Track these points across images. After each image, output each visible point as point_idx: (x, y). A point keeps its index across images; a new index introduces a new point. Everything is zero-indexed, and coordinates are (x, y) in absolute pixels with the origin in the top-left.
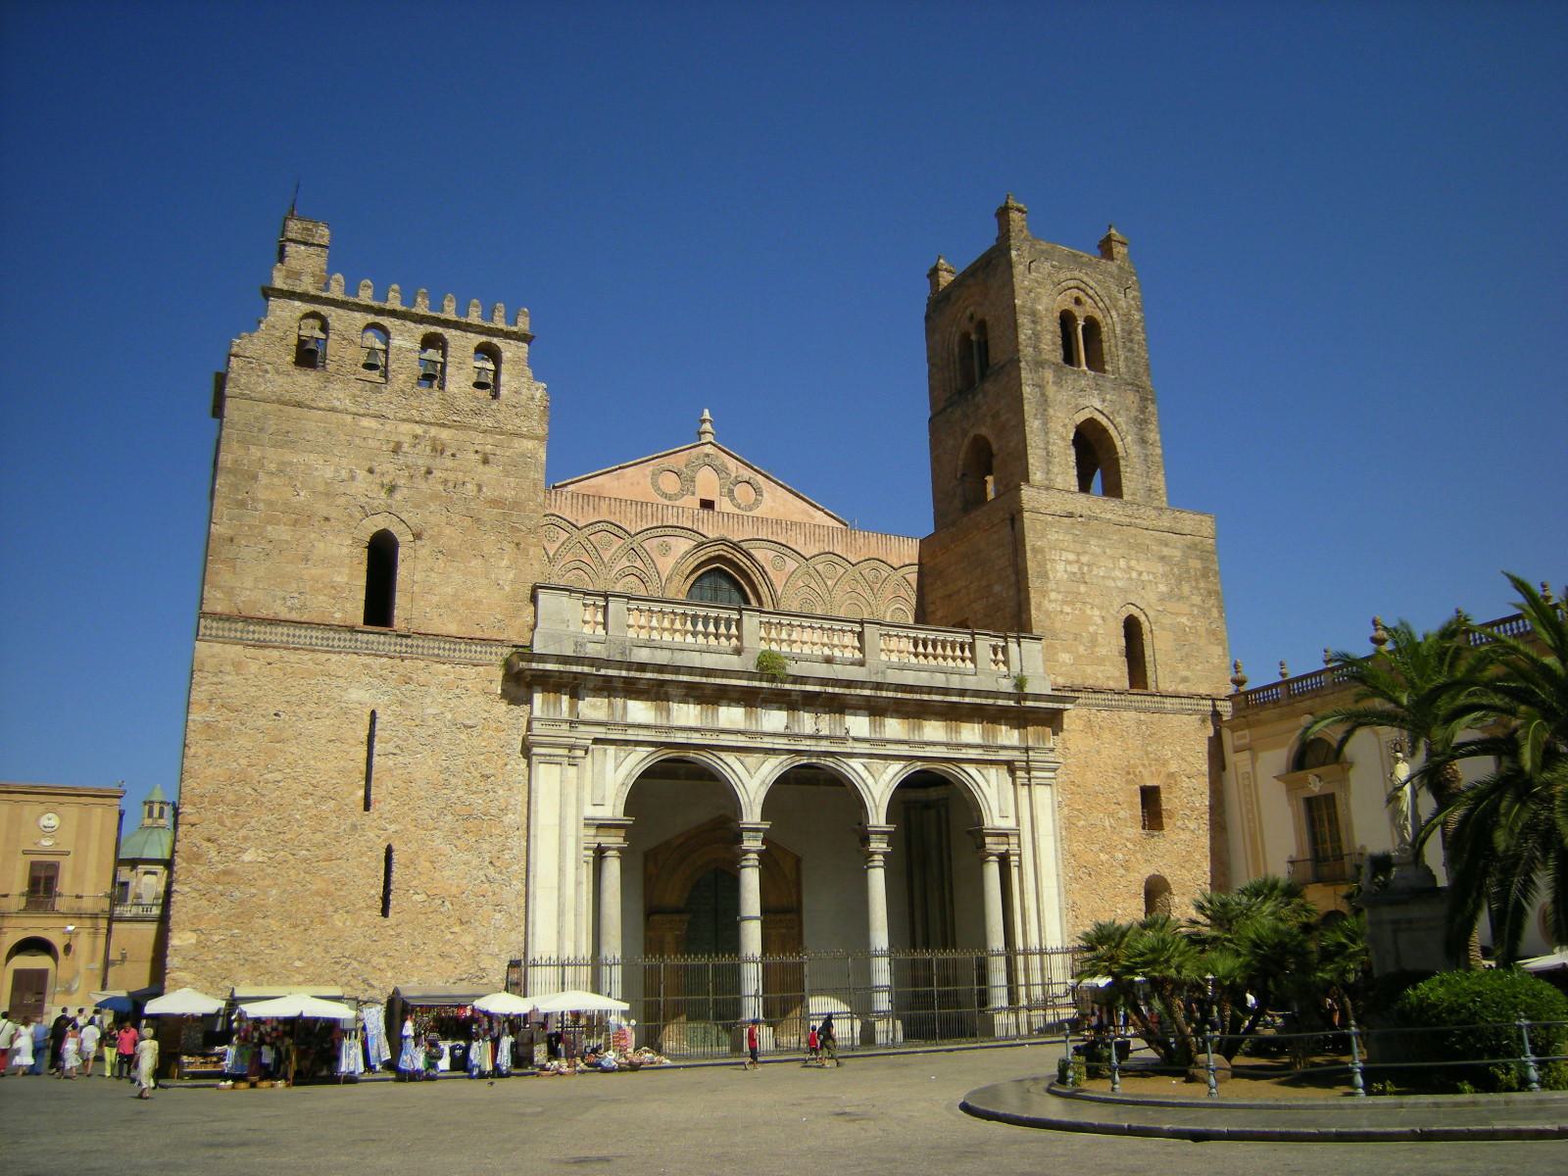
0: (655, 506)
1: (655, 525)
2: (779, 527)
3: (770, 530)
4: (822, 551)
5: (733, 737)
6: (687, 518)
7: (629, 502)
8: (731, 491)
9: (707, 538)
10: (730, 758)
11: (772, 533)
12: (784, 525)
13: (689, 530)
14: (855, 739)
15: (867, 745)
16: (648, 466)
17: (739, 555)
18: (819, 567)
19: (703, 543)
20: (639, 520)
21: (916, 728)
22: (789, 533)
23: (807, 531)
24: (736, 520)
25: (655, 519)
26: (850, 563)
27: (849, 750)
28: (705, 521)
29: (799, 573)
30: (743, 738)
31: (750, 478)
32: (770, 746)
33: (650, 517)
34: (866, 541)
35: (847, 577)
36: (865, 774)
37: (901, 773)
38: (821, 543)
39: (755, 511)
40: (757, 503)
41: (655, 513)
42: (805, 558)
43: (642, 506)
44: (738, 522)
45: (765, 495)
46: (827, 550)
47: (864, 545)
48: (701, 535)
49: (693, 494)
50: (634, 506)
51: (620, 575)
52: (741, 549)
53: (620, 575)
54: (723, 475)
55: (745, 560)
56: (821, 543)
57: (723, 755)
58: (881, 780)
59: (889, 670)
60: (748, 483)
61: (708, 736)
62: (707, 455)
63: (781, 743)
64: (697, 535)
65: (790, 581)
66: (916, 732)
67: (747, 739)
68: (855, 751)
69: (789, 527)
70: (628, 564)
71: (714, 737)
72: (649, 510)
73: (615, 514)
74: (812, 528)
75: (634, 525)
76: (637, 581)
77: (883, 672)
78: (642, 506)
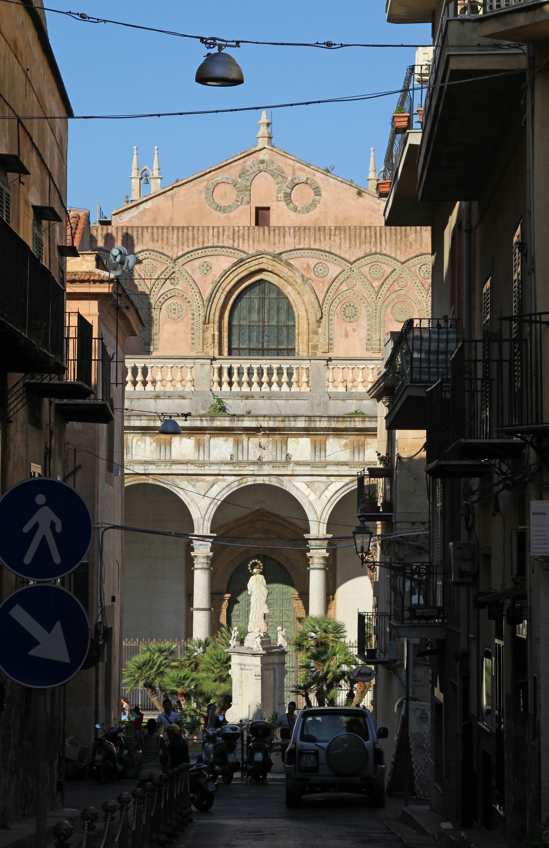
0: (196, 228)
1: (196, 247)
2: (322, 233)
3: (313, 238)
4: (368, 251)
5: (184, 467)
6: (228, 236)
7: (171, 228)
8: (288, 196)
9: (248, 254)
10: (183, 483)
11: (315, 240)
12: (327, 231)
13: (229, 248)
14: (298, 463)
15: (308, 468)
16: (201, 182)
17: (279, 266)
18: (365, 270)
19: (242, 260)
20: (180, 245)
21: (356, 451)
22: (333, 237)
23: (353, 233)
24: (277, 232)
25: (196, 242)
26: (398, 261)
27: (290, 473)
28: (246, 237)
29: (342, 278)
30: (192, 467)
31: (307, 179)
32: (217, 472)
33: (191, 241)
34: (419, 236)
35: (394, 276)
36: (307, 491)
37: (343, 490)
38: (367, 245)
39: (311, 213)
40: (314, 204)
41: (196, 236)
42: (349, 262)
43: (183, 231)
44: (279, 234)
45: (323, 194)
46: (373, 251)
47: (415, 241)
48: (241, 251)
49: (249, 203)
50: (175, 232)
51: (163, 298)
52: (281, 260)
53: (163, 298)
54: (280, 179)
55: (286, 270)
56: (367, 245)
57: (177, 480)
58: (323, 496)
59: (331, 402)
60: (306, 183)
61: (162, 467)
62: (262, 162)
63: (226, 469)
64: (237, 252)
65: (333, 286)
66: (356, 454)
67: (197, 468)
68: (295, 473)
69: (333, 232)
70: (171, 287)
71: (168, 467)
72: (190, 234)
73: (157, 241)
74: (358, 231)
75: (175, 249)
76: (179, 302)
77: (326, 404)
78: (183, 231)
